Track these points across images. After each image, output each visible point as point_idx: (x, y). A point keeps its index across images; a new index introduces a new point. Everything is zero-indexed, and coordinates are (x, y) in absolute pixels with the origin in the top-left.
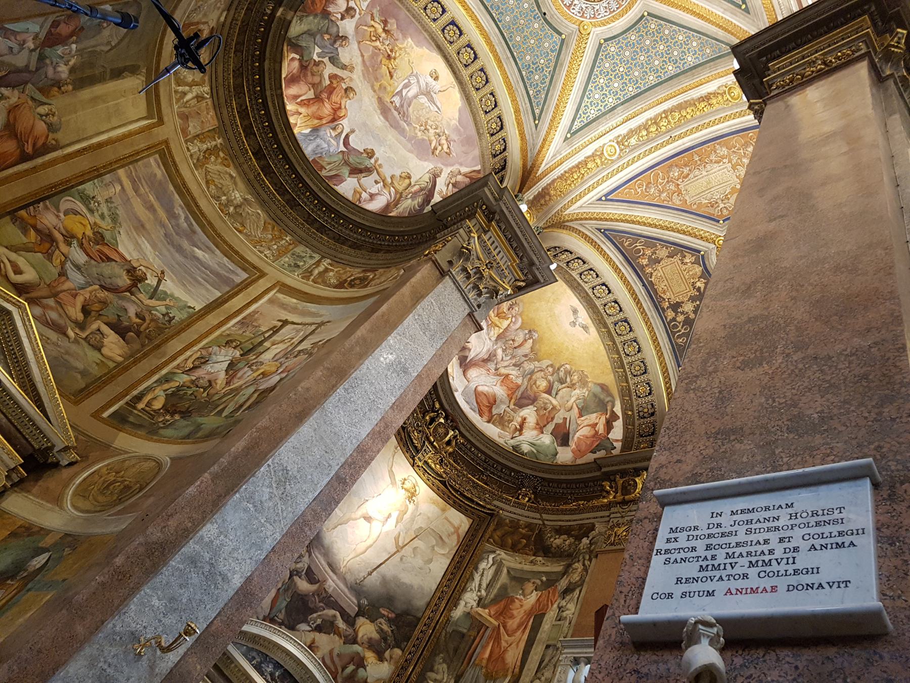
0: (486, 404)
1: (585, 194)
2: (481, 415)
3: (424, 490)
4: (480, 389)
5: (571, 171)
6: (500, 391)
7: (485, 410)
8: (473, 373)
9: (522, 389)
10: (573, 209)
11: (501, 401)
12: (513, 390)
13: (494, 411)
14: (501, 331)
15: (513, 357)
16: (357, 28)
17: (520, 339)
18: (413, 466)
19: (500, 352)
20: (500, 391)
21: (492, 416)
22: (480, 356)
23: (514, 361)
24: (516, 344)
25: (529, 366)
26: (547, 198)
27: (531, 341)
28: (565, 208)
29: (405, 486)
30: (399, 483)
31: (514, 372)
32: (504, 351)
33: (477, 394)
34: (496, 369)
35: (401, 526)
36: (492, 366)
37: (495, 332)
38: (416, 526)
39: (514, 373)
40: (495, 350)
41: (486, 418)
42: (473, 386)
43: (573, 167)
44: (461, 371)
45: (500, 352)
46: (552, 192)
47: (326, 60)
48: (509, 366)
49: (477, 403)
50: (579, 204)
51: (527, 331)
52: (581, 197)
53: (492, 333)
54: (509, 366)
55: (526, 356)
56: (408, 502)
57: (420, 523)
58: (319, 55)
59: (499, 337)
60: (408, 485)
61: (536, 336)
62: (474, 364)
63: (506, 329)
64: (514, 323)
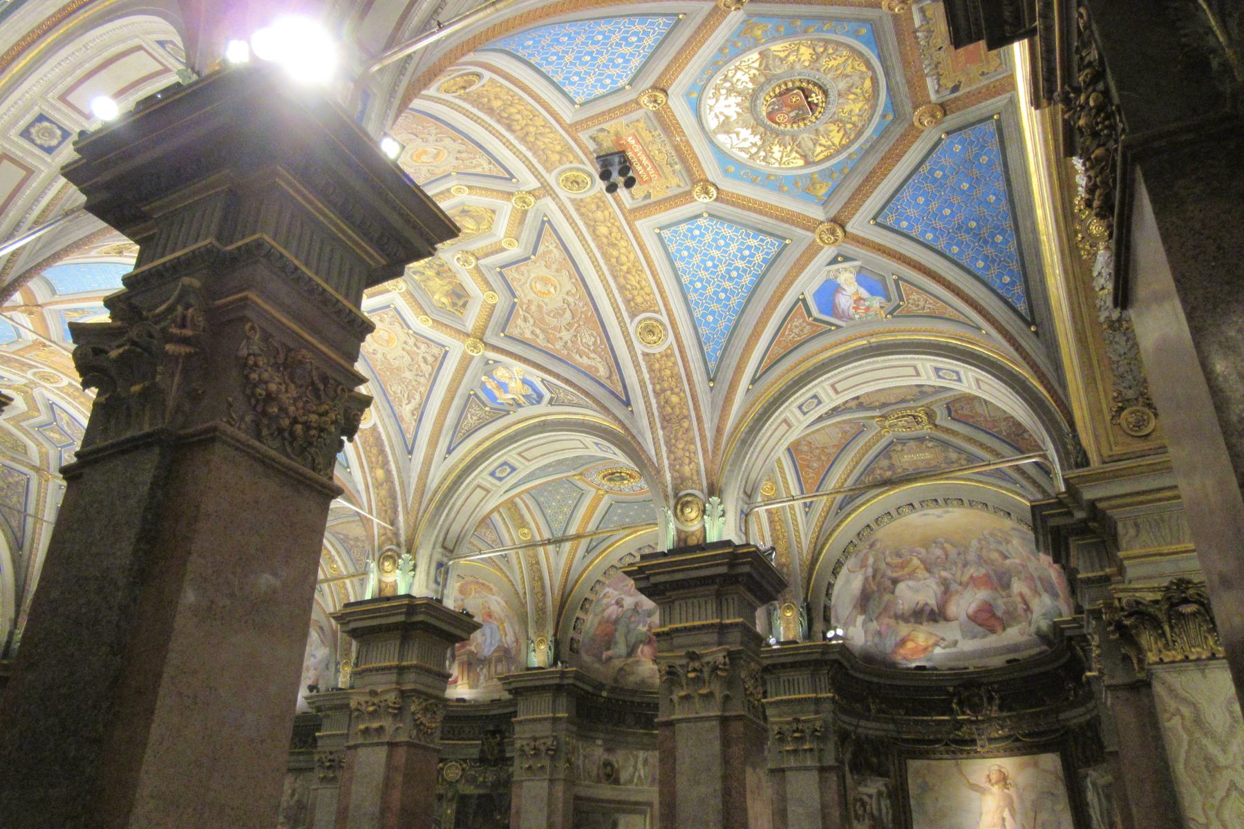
0: (987, 619)
1: (797, 526)
2: (993, 631)
3: (1007, 764)
4: (971, 611)
5: (773, 529)
6: (982, 595)
7: (993, 622)
8: (952, 609)
9: (991, 573)
10: (806, 544)
11: (994, 600)
12: (986, 581)
13: (999, 614)
14: (922, 566)
15: (955, 564)
16: (631, 595)
17: (938, 552)
18: (984, 758)
19: (944, 574)
20: (982, 595)
21: (1002, 620)
22: (939, 593)
23: (960, 565)
24: (944, 557)
25: (972, 556)
26: (785, 570)
27: (946, 545)
28: (800, 553)
29: (993, 781)
30: (987, 785)
31: (972, 570)
32: (945, 569)
33: (973, 618)
34: (961, 584)
35: (1018, 817)
36: (954, 587)
37: (921, 573)
38: (1028, 804)
39: (972, 571)
40: (940, 577)
41: (999, 629)
42: (963, 617)
43: (770, 526)
44: (942, 624)
45: (944, 574)
46: (783, 560)
47: (649, 620)
48: (963, 572)
49: (980, 625)
50: (802, 536)
51: (934, 545)
52: (798, 531)
53: (920, 576)
54: (963, 572)
55: (959, 554)
56: (1006, 791)
57: (1030, 796)
58: (644, 626)
59: (928, 570)
60: (994, 777)
61: (941, 540)
62: (942, 606)
63: (923, 561)
64: (919, 553)
